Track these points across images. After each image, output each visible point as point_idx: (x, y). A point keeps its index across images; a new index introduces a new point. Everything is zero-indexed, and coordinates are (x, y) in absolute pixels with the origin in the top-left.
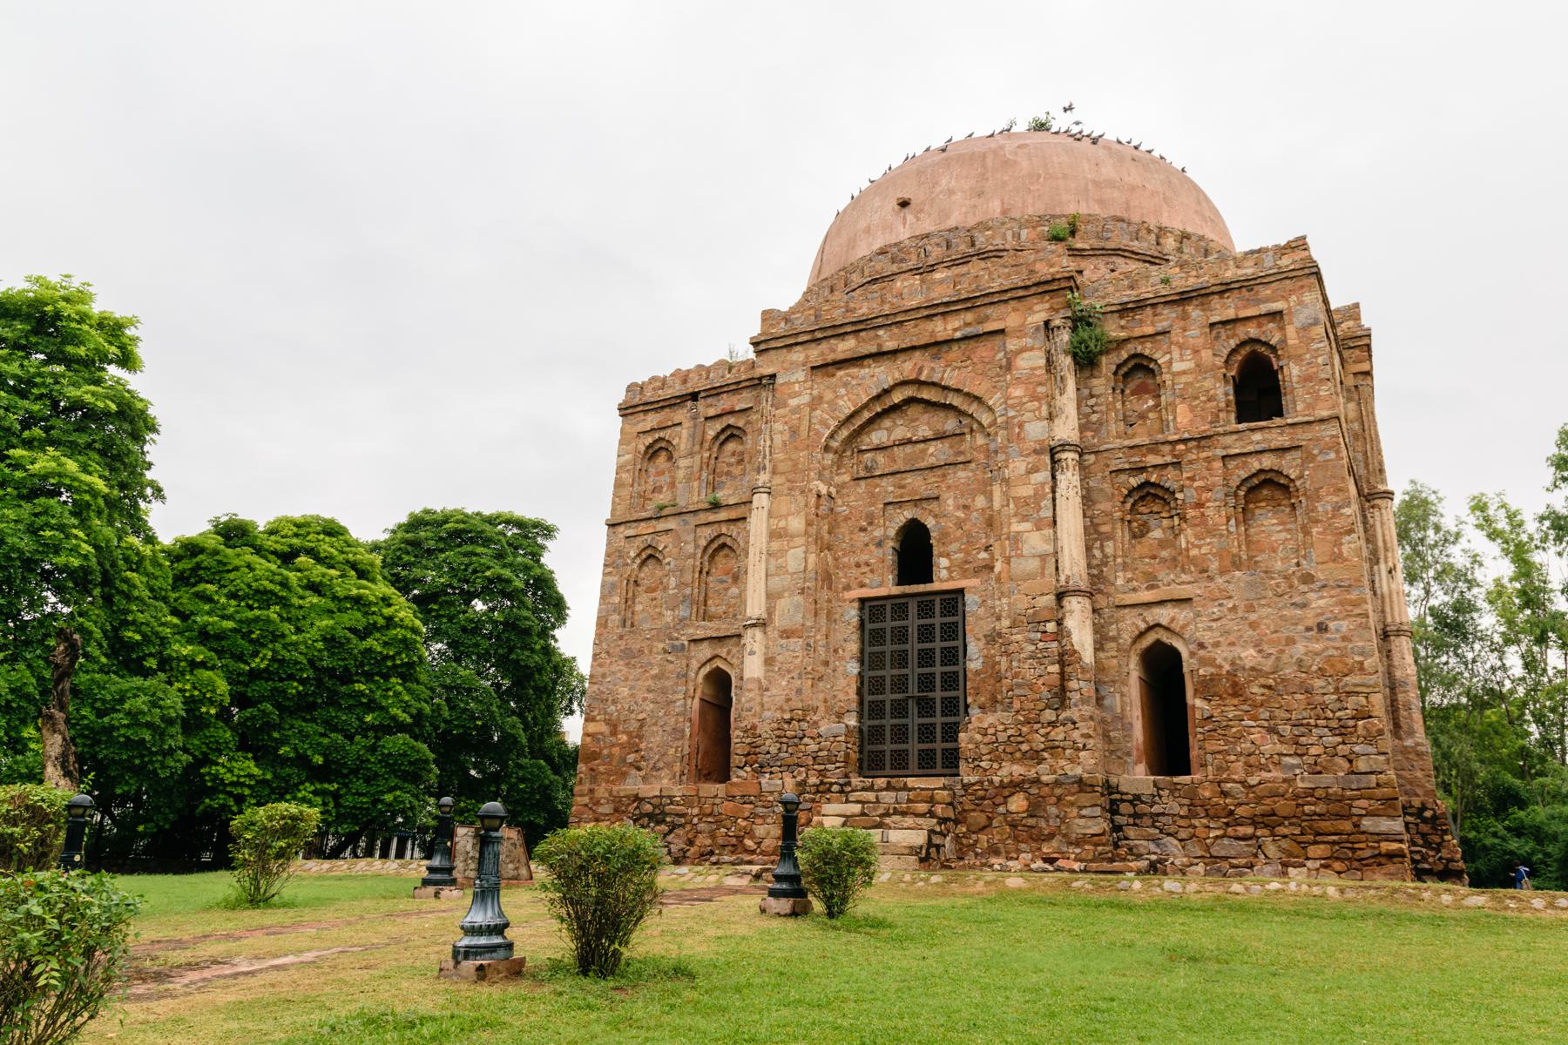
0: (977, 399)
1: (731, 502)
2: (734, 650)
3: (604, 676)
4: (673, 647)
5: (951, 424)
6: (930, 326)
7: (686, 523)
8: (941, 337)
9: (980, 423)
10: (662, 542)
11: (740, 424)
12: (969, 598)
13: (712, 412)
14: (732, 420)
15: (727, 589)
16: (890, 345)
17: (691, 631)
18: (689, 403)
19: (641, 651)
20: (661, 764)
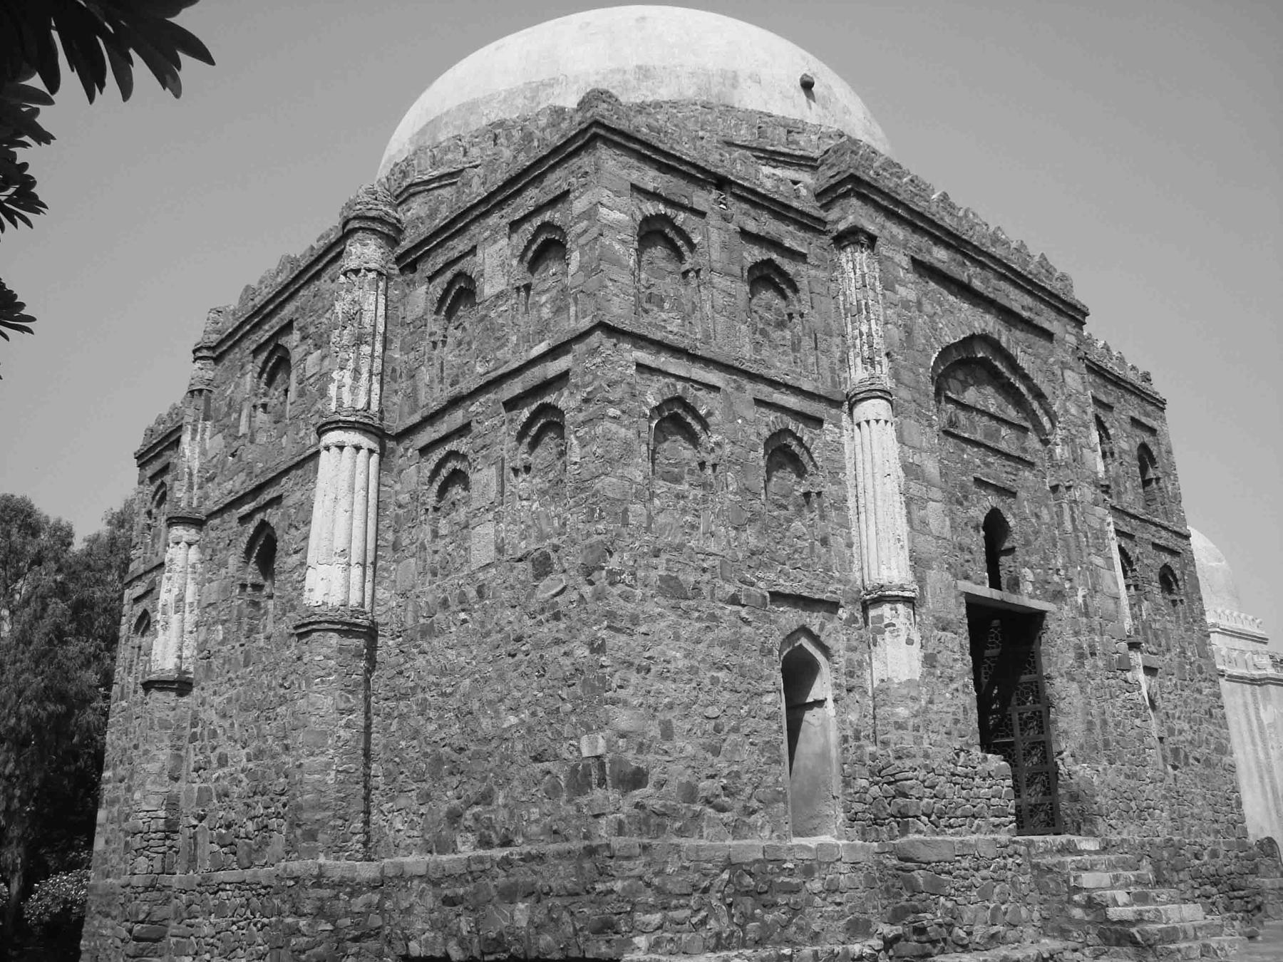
0: (1039, 396)
1: (805, 388)
2: (829, 626)
3: (635, 620)
4: (748, 596)
5: (1012, 413)
6: (1003, 285)
7: (739, 388)
8: (1016, 307)
9: (1038, 427)
10: (705, 403)
11: (788, 266)
12: (1051, 624)
13: (751, 227)
14: (774, 256)
15: (789, 521)
16: (977, 284)
17: (772, 576)
18: (715, 194)
19: (696, 588)
20: (755, 804)
